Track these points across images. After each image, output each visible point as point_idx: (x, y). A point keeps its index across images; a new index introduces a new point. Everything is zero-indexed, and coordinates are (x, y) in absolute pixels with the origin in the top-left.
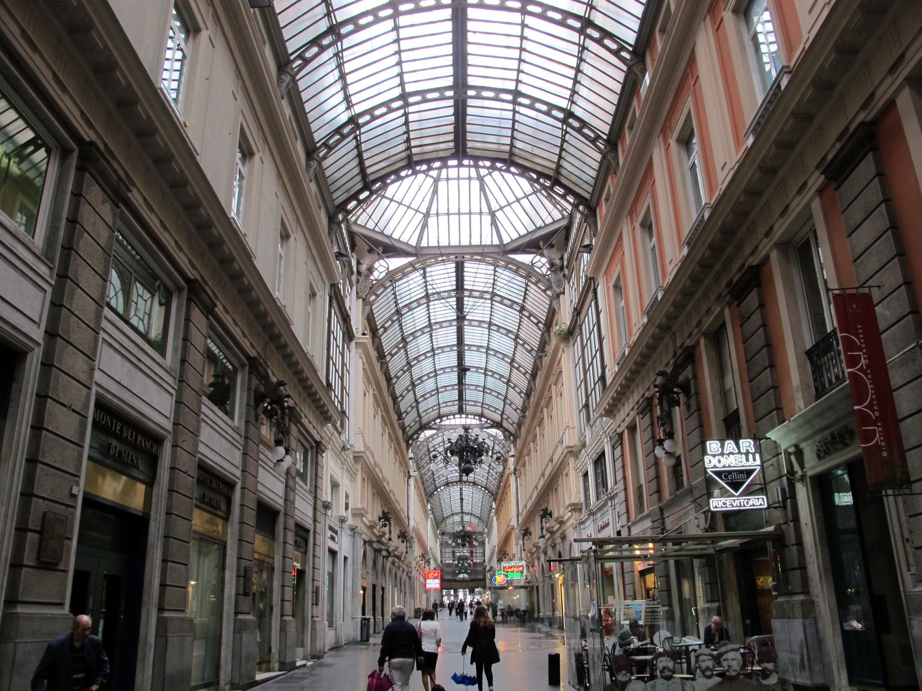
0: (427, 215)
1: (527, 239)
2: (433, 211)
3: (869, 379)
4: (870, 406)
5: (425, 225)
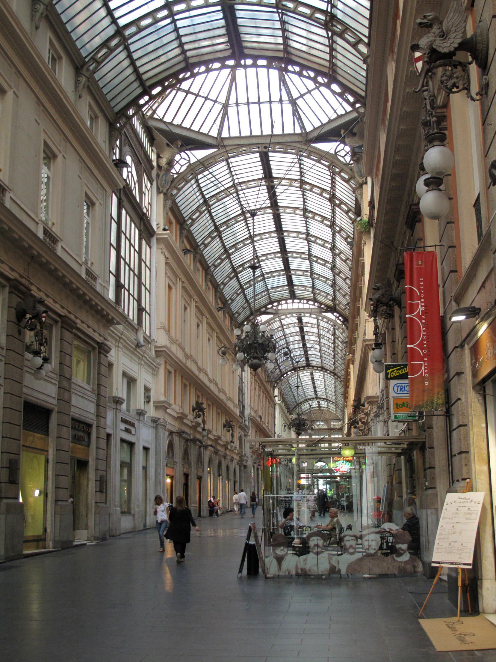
0: (226, 106)
2: (232, 100)
3: (422, 323)
4: (421, 346)
5: (225, 114)
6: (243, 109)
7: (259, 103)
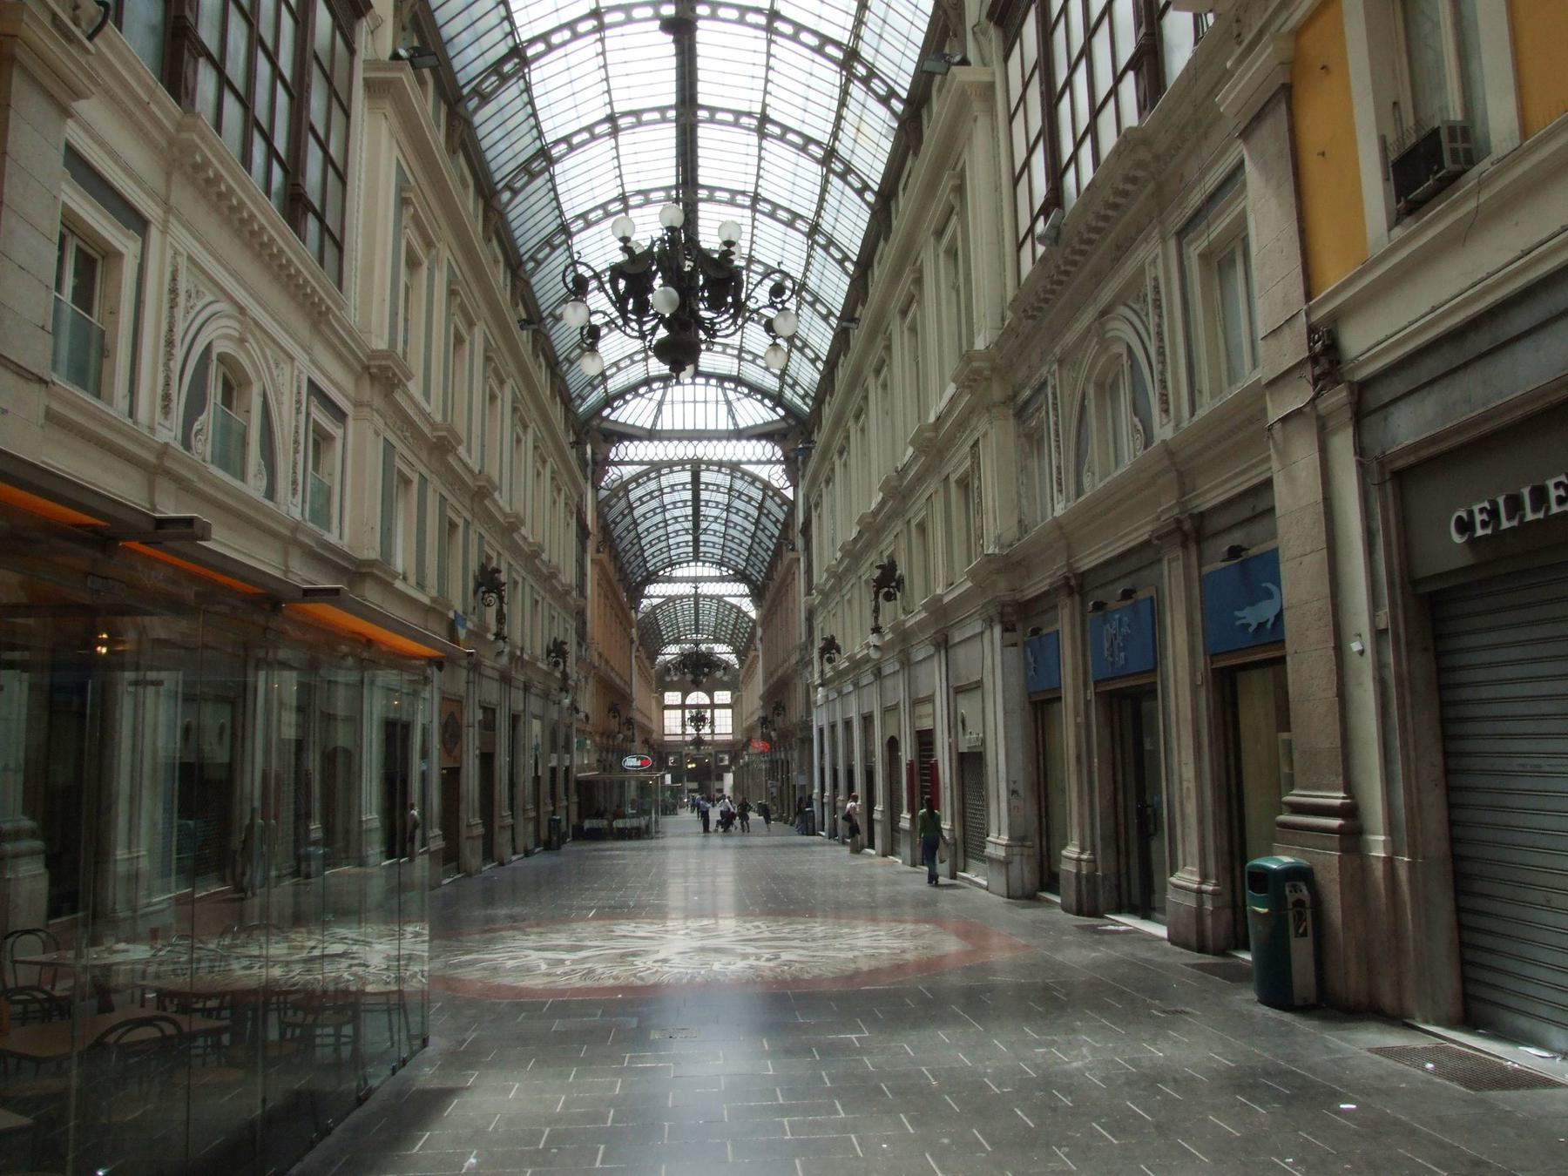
0: (660, 404)
1: (766, 429)
5: (659, 411)
6: (678, 408)
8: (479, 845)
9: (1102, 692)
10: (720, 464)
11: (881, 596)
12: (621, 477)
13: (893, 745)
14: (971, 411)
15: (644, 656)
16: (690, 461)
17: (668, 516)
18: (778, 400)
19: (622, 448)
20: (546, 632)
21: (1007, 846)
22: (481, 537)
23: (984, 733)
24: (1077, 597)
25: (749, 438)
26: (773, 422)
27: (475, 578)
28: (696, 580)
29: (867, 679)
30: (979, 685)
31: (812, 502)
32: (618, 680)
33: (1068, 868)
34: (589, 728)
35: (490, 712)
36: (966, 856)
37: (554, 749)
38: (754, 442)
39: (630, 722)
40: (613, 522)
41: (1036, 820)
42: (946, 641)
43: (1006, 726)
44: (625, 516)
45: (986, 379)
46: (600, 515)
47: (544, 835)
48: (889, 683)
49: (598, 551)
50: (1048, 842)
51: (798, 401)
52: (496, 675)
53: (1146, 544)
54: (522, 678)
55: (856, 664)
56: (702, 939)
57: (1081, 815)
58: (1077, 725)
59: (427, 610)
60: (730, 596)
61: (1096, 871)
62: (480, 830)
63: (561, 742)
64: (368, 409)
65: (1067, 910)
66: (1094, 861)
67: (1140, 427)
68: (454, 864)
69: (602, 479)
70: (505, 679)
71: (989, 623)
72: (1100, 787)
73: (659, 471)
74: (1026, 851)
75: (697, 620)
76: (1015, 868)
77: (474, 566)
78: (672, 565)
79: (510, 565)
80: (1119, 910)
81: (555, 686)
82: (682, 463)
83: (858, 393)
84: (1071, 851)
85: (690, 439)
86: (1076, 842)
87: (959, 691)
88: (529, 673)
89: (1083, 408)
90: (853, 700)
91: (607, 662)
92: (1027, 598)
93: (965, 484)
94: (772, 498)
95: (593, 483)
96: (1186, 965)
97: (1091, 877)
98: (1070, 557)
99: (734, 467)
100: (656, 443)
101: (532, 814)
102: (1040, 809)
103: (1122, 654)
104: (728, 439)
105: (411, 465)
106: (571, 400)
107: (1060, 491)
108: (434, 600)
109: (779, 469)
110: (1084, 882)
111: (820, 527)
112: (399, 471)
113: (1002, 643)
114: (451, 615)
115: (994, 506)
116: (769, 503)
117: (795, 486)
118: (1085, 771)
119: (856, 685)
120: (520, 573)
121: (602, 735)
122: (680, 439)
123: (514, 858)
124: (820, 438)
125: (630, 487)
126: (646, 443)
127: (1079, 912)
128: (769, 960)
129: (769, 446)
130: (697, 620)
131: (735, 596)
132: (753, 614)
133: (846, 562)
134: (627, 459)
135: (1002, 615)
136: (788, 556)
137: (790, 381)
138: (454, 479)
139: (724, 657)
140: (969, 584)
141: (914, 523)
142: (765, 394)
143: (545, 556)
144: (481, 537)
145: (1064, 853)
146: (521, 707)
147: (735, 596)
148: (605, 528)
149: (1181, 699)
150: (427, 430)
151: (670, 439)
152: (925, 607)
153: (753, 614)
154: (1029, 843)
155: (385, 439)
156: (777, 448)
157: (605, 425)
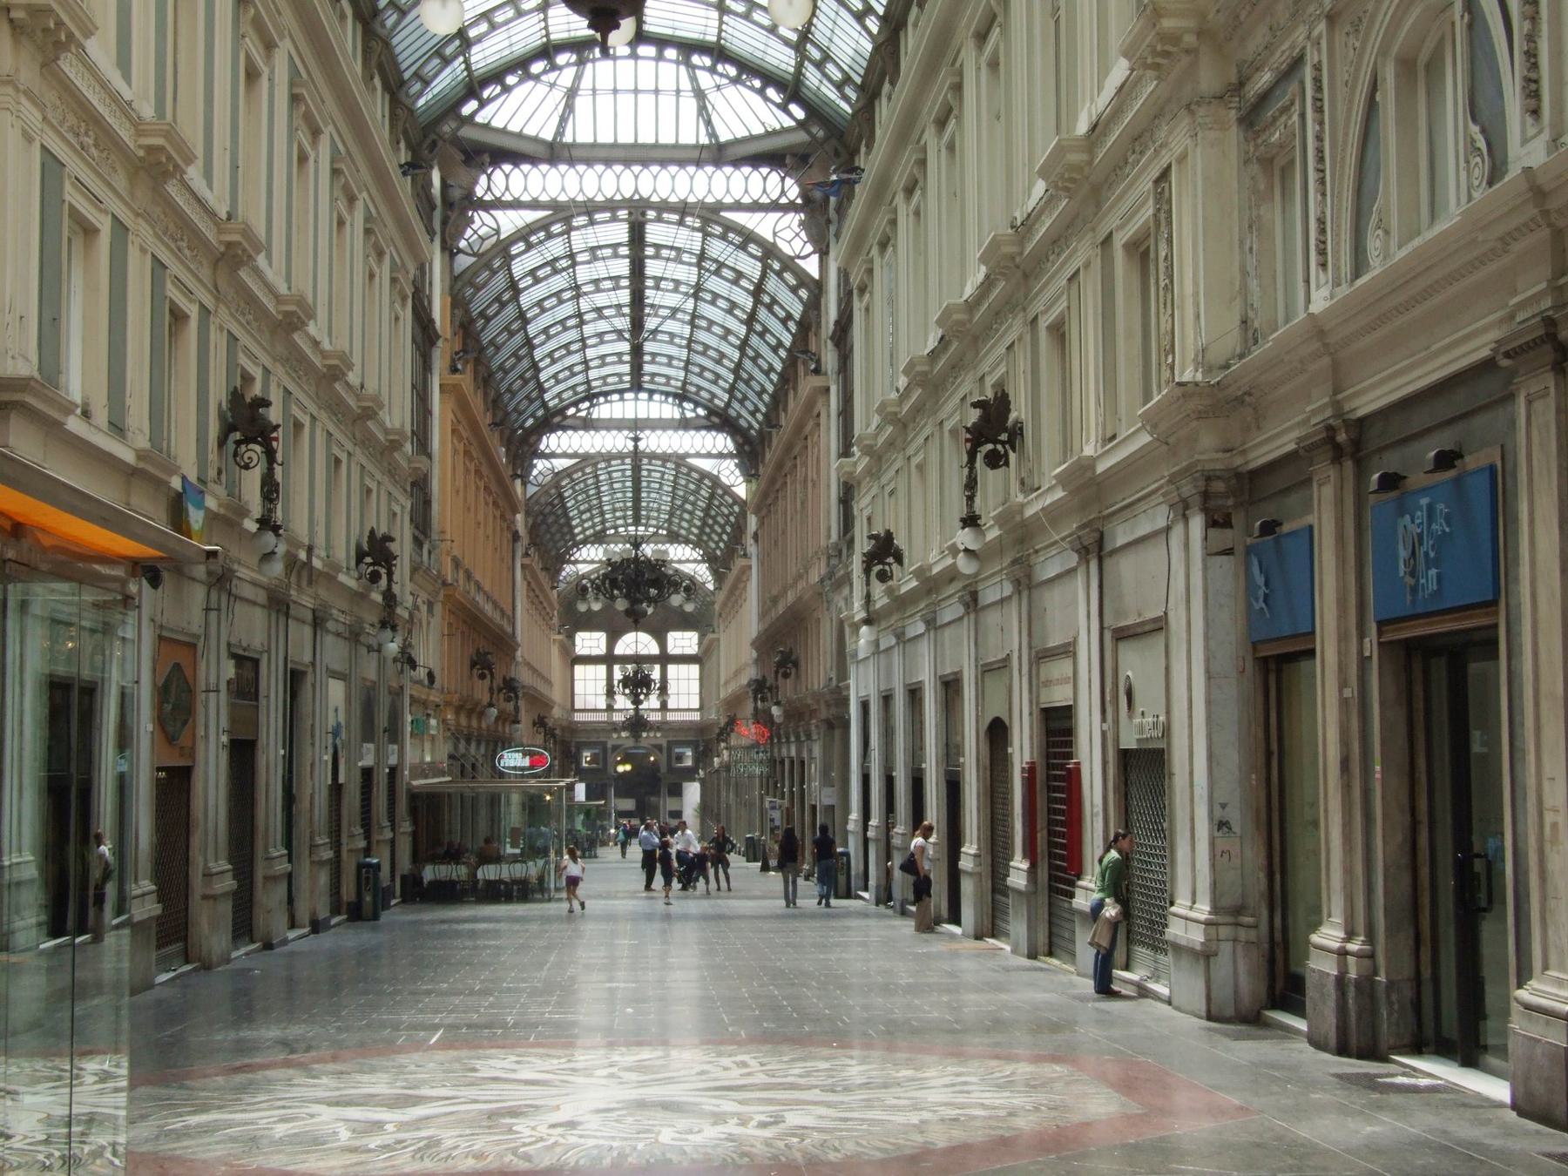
0: (572, 93)
5: (569, 107)
6: (605, 101)
7: (636, 91)
8: (226, 908)
9: (1391, 642)
10: (683, 209)
11: (979, 457)
12: (498, 232)
13: (997, 733)
14: (1158, 114)
15: (537, 566)
16: (628, 203)
17: (585, 305)
18: (792, 89)
19: (498, 176)
20: (355, 515)
21: (1208, 923)
22: (233, 339)
23: (1168, 712)
24: (1349, 464)
25: (737, 163)
26: (784, 131)
27: (221, 415)
28: (636, 426)
29: (951, 610)
30: (1159, 626)
31: (855, 281)
32: (488, 608)
33: (1321, 966)
34: (435, 697)
35: (247, 663)
36: (1129, 941)
37: (368, 734)
38: (747, 170)
39: (510, 687)
40: (482, 314)
41: (1262, 875)
42: (1100, 542)
43: (1209, 702)
44: (503, 305)
45: (1187, 52)
46: (458, 302)
47: (348, 891)
48: (992, 619)
49: (454, 370)
50: (1284, 918)
51: (831, 93)
52: (261, 597)
53: (1486, 367)
54: (308, 602)
55: (931, 585)
56: (641, 1084)
57: (1348, 871)
58: (1344, 703)
59: (131, 474)
60: (698, 455)
61: (1376, 973)
62: (228, 883)
63: (382, 720)
64: (10, 90)
65: (1318, 1043)
66: (1371, 956)
67: (1481, 143)
68: (178, 946)
69: (460, 234)
70: (278, 604)
71: (1182, 510)
72: (1385, 815)
73: (567, 220)
74: (1243, 934)
75: (637, 500)
76: (1223, 965)
77: (218, 394)
78: (591, 397)
79: (287, 392)
80: (1417, 1049)
81: (371, 617)
82: (611, 206)
83: (944, 79)
84: (1329, 935)
85: (627, 163)
86: (1338, 918)
87: (1123, 635)
88: (322, 593)
89: (1372, 106)
90: (924, 649)
91: (469, 576)
92: (1252, 466)
93: (1141, 252)
94: (779, 274)
95: (443, 241)
96: (1549, 1155)
97: (1366, 985)
98: (1337, 390)
99: (708, 215)
100: (563, 168)
101: (327, 854)
102: (1270, 857)
103: (1433, 572)
104: (699, 163)
105: (96, 200)
106: (402, 83)
107: (1323, 265)
108: (141, 455)
109: (793, 220)
110: (1351, 993)
111: (868, 332)
112: (74, 212)
113: (1205, 548)
114: (176, 483)
115: (1196, 294)
116: (772, 284)
117: (823, 253)
118: (1357, 793)
119: (931, 623)
120: (306, 406)
121: (458, 710)
122: (608, 162)
123: (291, 935)
124: (871, 162)
125: (515, 250)
126: (544, 167)
127: (1342, 1050)
128: (763, 1125)
129: (774, 177)
130: (637, 500)
131: (709, 455)
132: (741, 490)
133: (917, 393)
134: (508, 197)
135: (1206, 496)
136: (807, 384)
137: (816, 54)
138: (180, 230)
139: (687, 568)
140: (1145, 438)
141: (1043, 324)
142: (769, 78)
143: (353, 378)
144: (233, 339)
145: (1315, 938)
146: (307, 658)
147: (709, 455)
148: (467, 328)
149: (1543, 657)
150: (125, 134)
151: (589, 162)
152: (1062, 480)
153: (741, 490)
154: (1248, 920)
155: (43, 146)
156: (789, 182)
157: (466, 132)
